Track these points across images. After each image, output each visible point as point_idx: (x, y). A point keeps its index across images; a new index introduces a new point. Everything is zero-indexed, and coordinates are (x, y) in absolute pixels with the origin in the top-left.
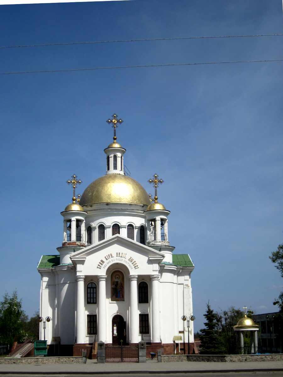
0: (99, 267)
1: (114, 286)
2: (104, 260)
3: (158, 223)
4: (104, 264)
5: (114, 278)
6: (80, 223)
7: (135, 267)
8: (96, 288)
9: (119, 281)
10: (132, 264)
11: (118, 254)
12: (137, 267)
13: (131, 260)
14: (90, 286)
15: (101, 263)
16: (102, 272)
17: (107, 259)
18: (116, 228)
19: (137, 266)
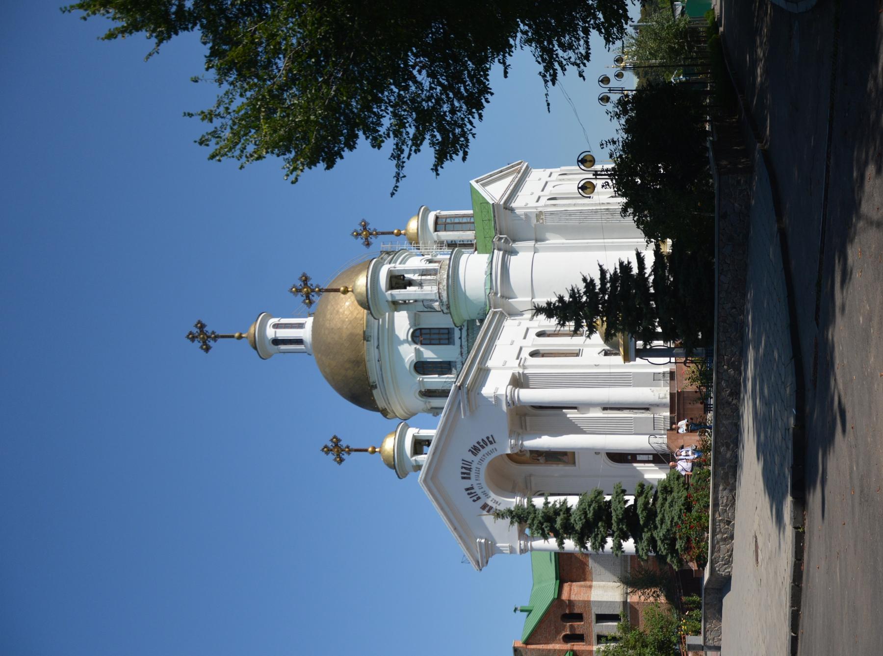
4: (490, 503)
7: (491, 443)
10: (483, 447)
11: (466, 476)
12: (491, 439)
13: (475, 450)
15: (487, 509)
17: (479, 498)
19: (488, 438)
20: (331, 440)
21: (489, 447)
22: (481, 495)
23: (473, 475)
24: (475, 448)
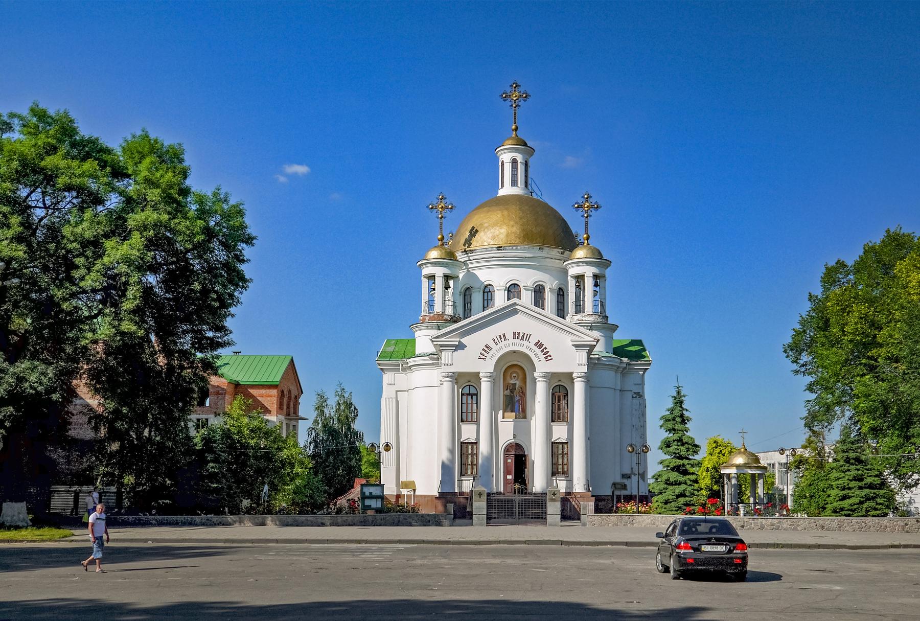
0: (482, 357)
1: (508, 392)
2: (492, 345)
3: (589, 283)
5: (508, 378)
6: (451, 283)
7: (546, 358)
8: (476, 395)
9: (518, 384)
11: (516, 335)
13: (539, 345)
14: (466, 391)
16: (486, 368)
18: (513, 290)
20: (596, 203)
21: (542, 357)
22: (499, 345)
23: (518, 341)
24: (541, 345)
